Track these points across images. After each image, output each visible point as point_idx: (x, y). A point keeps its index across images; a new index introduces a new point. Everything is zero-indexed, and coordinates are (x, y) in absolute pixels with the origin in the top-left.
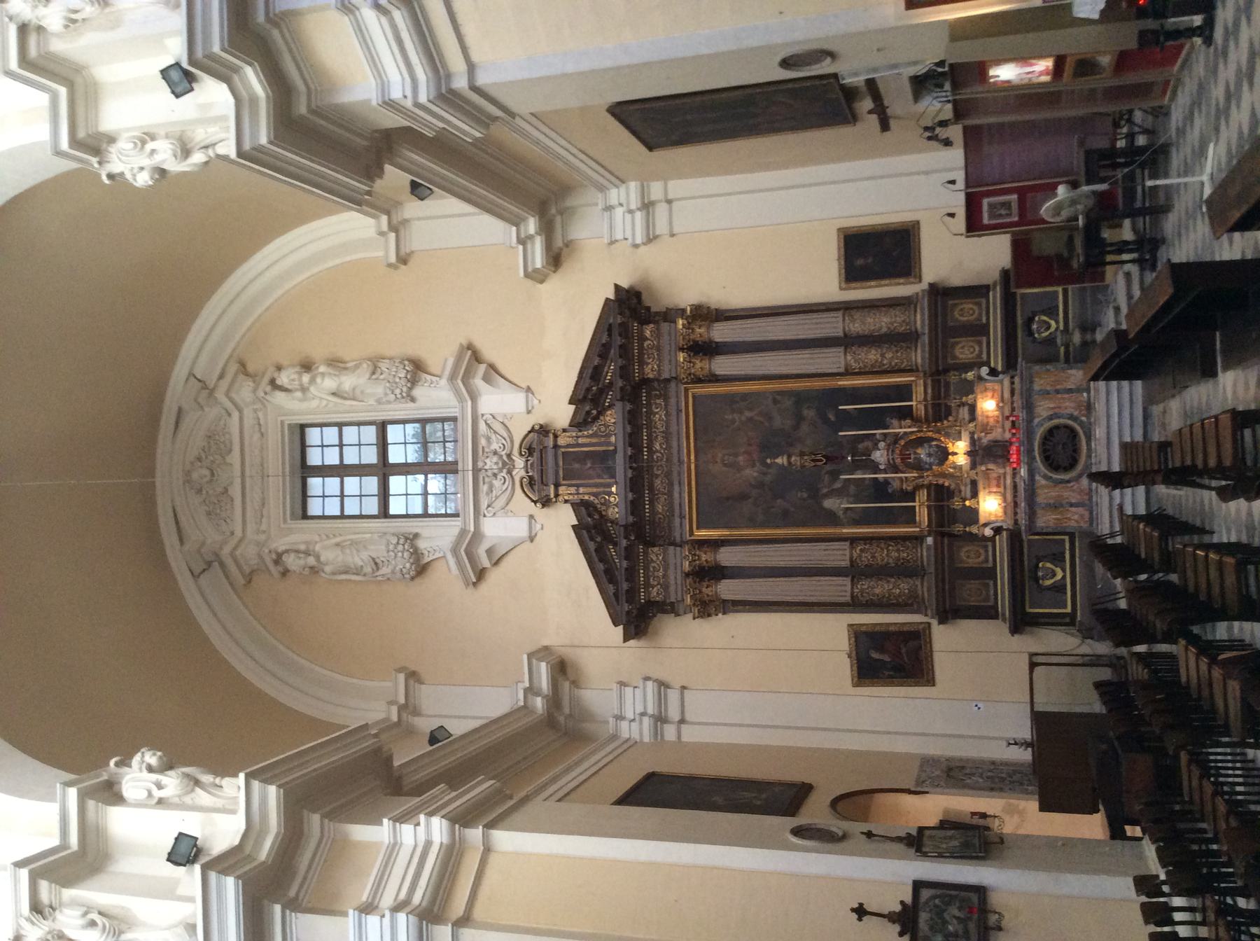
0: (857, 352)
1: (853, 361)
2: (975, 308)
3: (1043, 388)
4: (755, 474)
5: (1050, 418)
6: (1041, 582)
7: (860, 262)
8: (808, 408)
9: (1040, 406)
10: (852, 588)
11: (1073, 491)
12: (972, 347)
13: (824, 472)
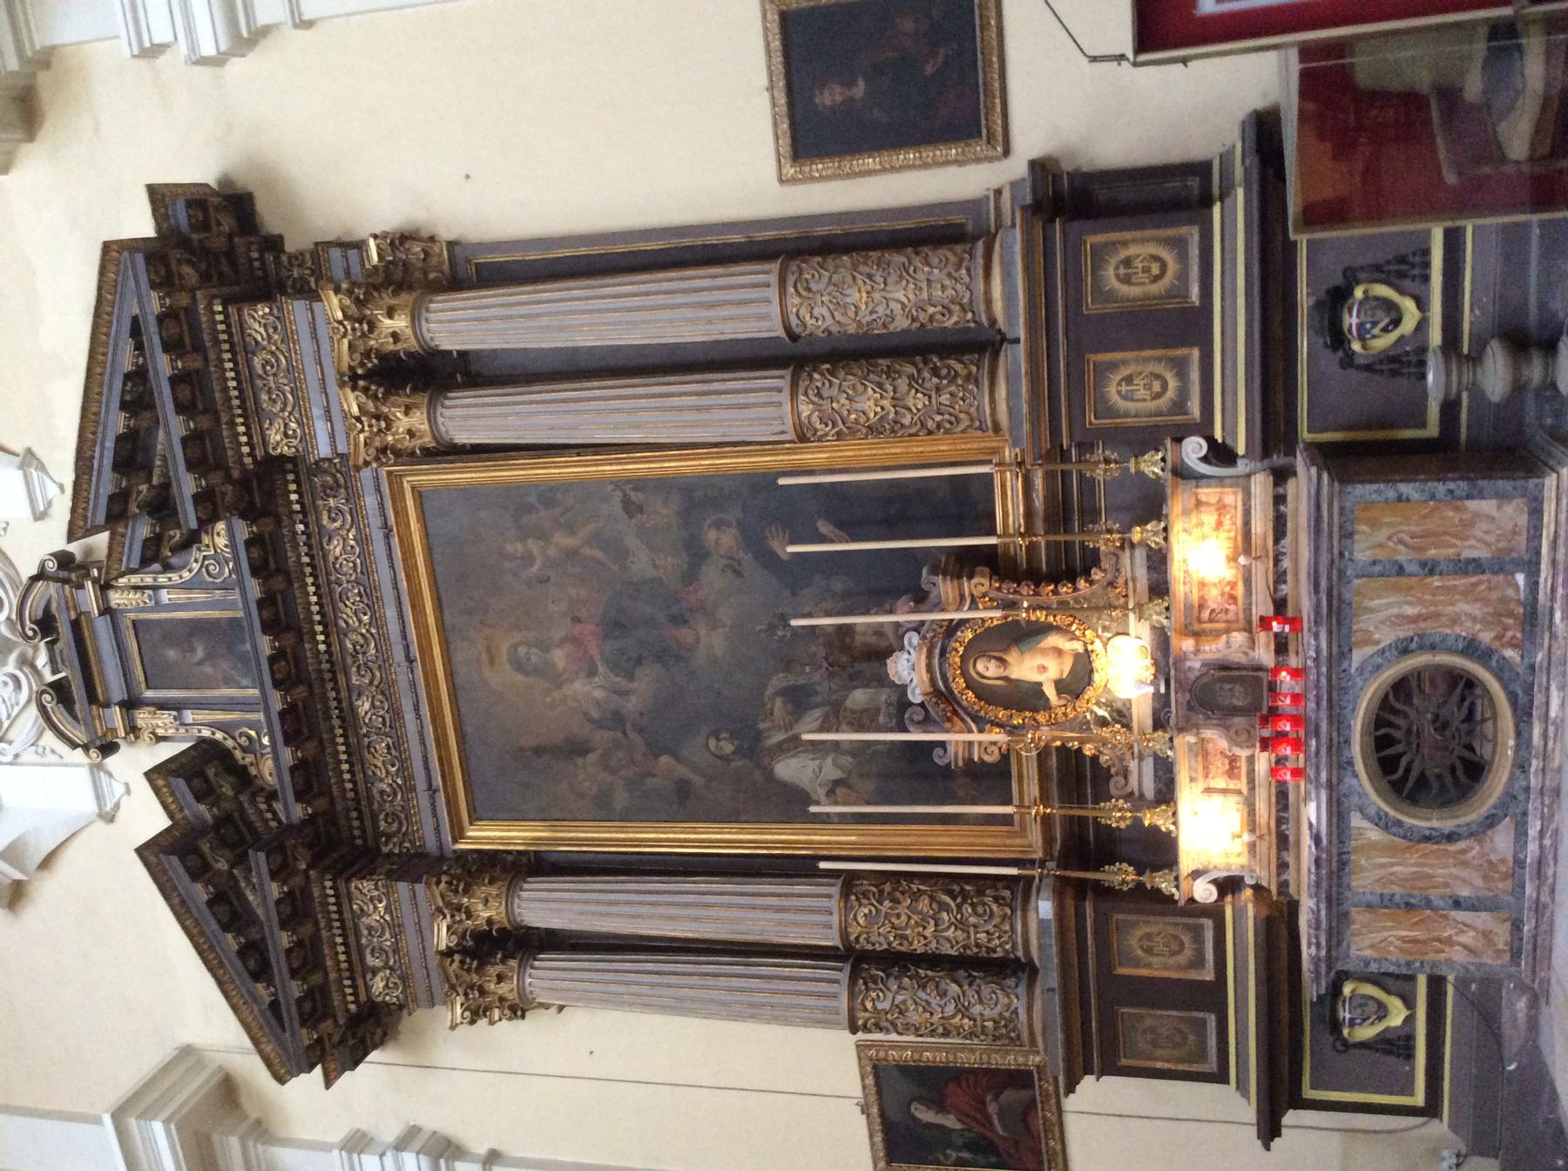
0: (825, 393)
1: (815, 418)
2: (1167, 256)
3: (1380, 554)
4: (598, 694)
5: (1404, 650)
6: (1346, 1032)
7: (829, 96)
8: (718, 525)
9: (1371, 610)
10: (851, 1011)
11: (1465, 864)
12: (1158, 377)
13: (769, 692)
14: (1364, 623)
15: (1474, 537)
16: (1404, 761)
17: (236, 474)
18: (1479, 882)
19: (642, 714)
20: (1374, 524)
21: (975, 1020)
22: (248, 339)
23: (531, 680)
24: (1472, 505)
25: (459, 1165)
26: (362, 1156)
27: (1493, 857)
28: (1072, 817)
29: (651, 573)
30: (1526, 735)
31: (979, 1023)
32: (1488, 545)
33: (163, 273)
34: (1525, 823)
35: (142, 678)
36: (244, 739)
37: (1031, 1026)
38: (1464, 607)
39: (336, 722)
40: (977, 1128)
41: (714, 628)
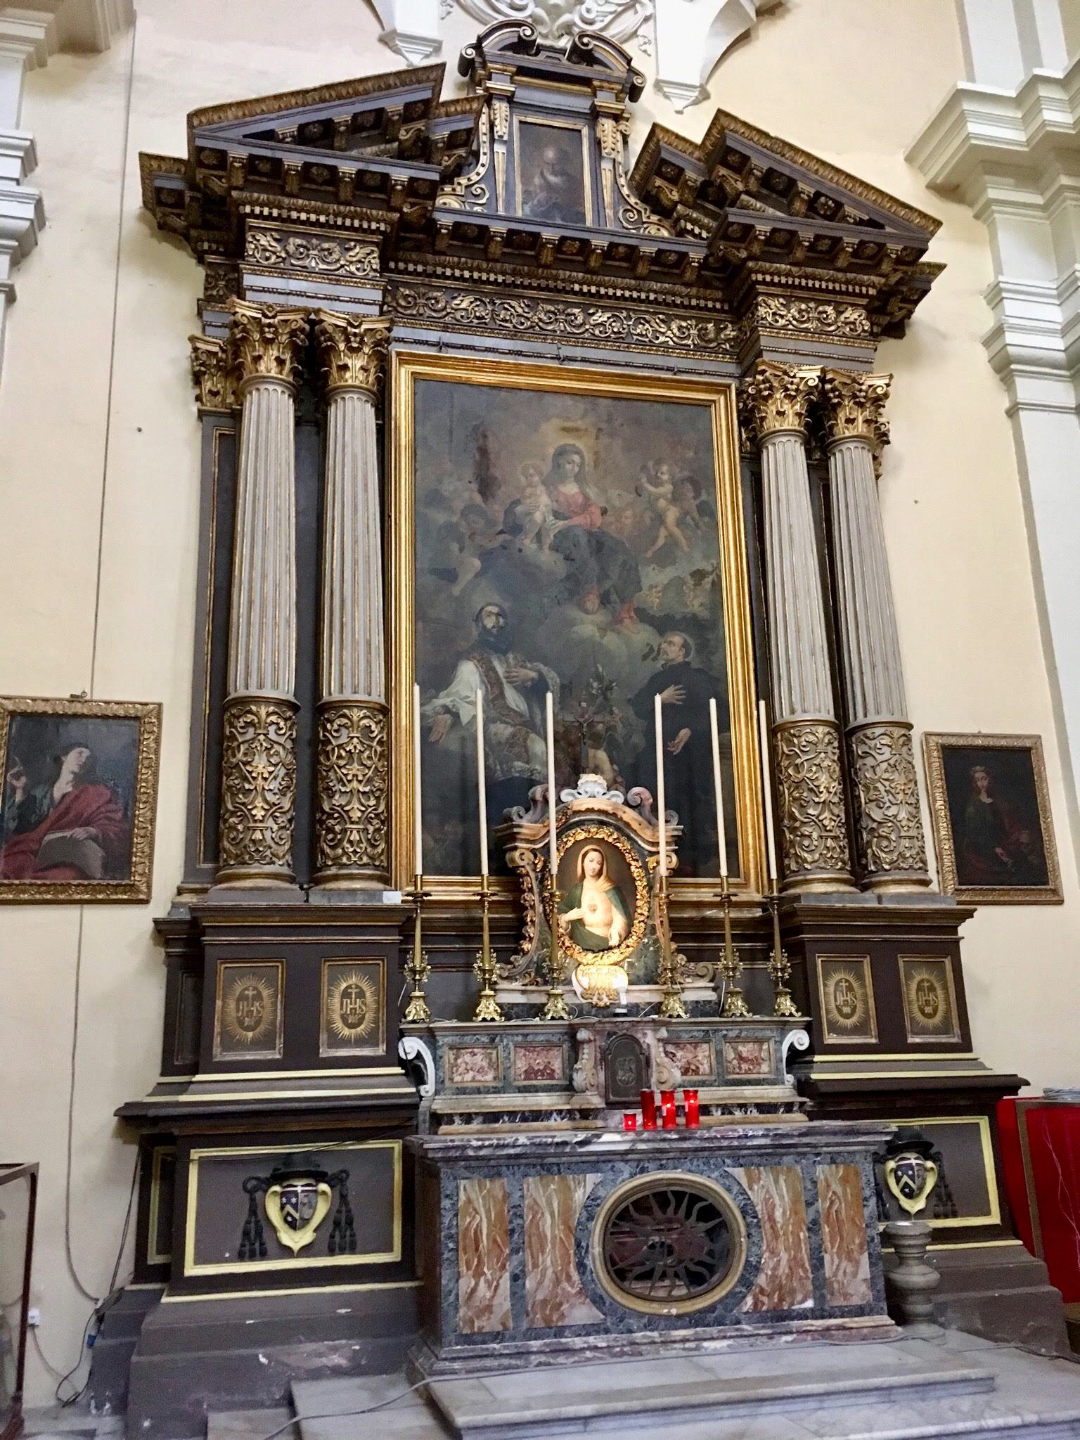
2: (938, 1018)
3: (821, 1186)
4: (538, 516)
6: (277, 1188)
7: (980, 777)
8: (685, 645)
9: (776, 1182)
10: (267, 701)
11: (557, 1282)
13: (544, 669)
14: (766, 1177)
15: (840, 1262)
16: (645, 1218)
17: (750, 264)
18: (540, 1297)
19: (520, 550)
20: (844, 1180)
21: (261, 821)
22: (845, 306)
23: (550, 460)
24: (865, 1259)
25: (5, 260)
26: (19, 161)
27: (565, 1307)
28: (481, 929)
29: (645, 583)
30: (679, 1323)
31: (259, 825)
32: (835, 1275)
33: (907, 259)
34: (598, 1333)
35: (529, 120)
36: (479, 191)
37: (249, 876)
38: (784, 1257)
39: (510, 279)
40: (53, 814)
41: (600, 629)
